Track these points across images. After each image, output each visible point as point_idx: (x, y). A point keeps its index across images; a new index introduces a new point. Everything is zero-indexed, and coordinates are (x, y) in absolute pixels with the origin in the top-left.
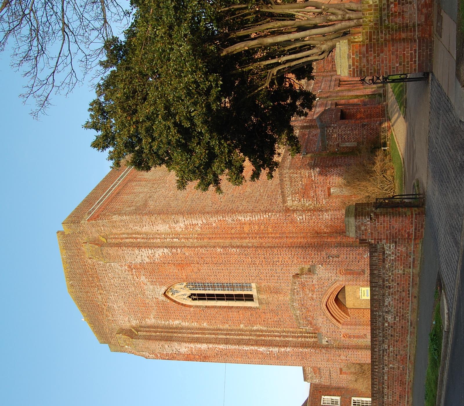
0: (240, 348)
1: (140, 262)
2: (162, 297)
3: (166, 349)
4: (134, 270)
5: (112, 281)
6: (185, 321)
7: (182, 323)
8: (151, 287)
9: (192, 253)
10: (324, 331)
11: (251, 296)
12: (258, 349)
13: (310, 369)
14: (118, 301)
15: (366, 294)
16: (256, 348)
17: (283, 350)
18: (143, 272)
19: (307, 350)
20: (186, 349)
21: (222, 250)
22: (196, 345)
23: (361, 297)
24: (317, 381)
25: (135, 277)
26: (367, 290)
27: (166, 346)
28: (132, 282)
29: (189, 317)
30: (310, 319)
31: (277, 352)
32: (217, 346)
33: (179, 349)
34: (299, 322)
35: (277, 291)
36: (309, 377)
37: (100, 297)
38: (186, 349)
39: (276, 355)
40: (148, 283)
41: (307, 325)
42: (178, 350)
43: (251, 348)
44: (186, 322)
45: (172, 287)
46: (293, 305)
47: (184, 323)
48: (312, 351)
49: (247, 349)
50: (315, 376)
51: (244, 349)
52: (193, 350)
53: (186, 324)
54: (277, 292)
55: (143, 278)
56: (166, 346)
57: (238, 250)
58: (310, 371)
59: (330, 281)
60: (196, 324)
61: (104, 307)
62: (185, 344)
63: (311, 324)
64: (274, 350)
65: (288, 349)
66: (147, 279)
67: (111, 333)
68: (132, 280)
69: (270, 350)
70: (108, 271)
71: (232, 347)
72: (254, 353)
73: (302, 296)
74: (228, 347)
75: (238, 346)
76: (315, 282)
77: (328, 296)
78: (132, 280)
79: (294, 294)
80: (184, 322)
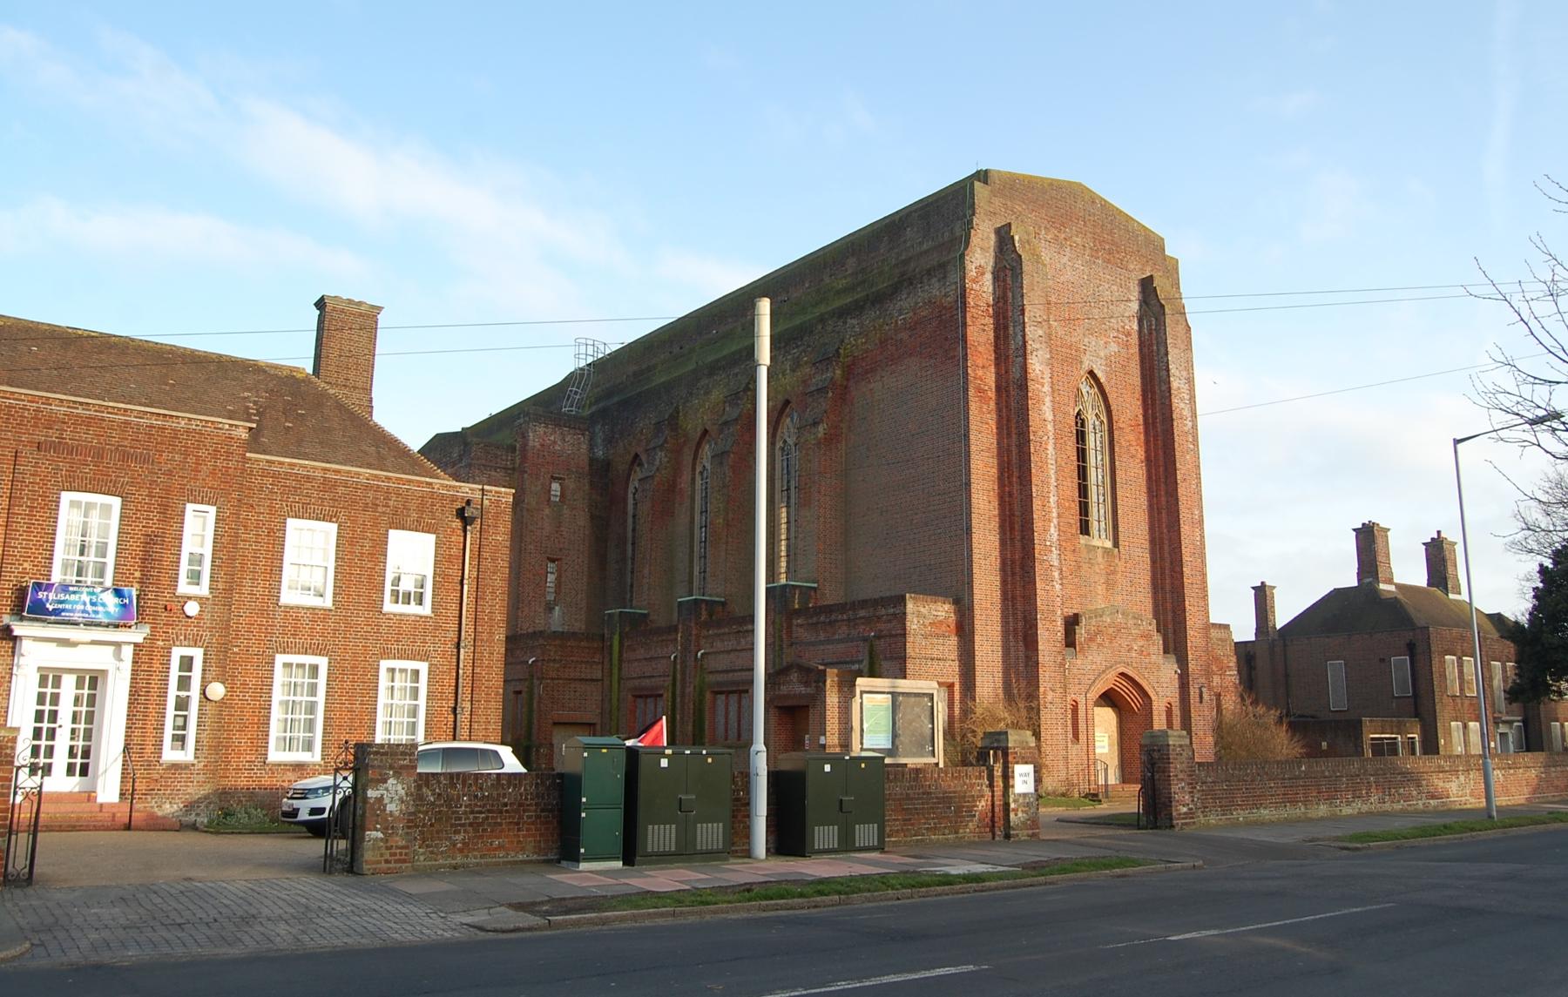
0: (1051, 488)
1: (1172, 371)
2: (1087, 365)
3: (1036, 328)
4: (1125, 339)
5: (1107, 286)
8: (1102, 354)
9: (1190, 467)
10: (1079, 662)
11: (1087, 533)
12: (1052, 525)
13: (939, 614)
14: (1074, 273)
16: (1055, 521)
17: (1056, 574)
18: (1123, 351)
19: (1059, 623)
21: (1197, 517)
24: (915, 627)
25: (1115, 334)
26: (1104, 747)
27: (1040, 332)
28: (1108, 323)
30: (1099, 640)
31: (1052, 563)
32: (1051, 441)
34: (1090, 618)
35: (1110, 585)
36: (922, 610)
37: (1079, 240)
39: (1045, 558)
40: (1107, 351)
41: (1088, 632)
42: (1035, 353)
43: (1054, 510)
45: (1096, 390)
46: (1117, 612)
48: (1059, 634)
49: (1051, 500)
50: (927, 622)
51: (1051, 495)
52: (1040, 387)
54: (1107, 583)
55: (1114, 348)
57: (1198, 543)
58: (936, 613)
59: (1156, 685)
61: (1063, 236)
63: (1091, 640)
64: (1055, 556)
65: (1058, 587)
66: (1113, 353)
67: (1015, 213)
68: (1111, 324)
69: (1054, 549)
70: (1120, 289)
71: (1053, 471)
72: (1044, 513)
73: (1133, 632)
74: (1052, 464)
75: (1055, 484)
76: (1154, 657)
77: (1137, 678)
78: (1111, 324)
79: (1135, 618)
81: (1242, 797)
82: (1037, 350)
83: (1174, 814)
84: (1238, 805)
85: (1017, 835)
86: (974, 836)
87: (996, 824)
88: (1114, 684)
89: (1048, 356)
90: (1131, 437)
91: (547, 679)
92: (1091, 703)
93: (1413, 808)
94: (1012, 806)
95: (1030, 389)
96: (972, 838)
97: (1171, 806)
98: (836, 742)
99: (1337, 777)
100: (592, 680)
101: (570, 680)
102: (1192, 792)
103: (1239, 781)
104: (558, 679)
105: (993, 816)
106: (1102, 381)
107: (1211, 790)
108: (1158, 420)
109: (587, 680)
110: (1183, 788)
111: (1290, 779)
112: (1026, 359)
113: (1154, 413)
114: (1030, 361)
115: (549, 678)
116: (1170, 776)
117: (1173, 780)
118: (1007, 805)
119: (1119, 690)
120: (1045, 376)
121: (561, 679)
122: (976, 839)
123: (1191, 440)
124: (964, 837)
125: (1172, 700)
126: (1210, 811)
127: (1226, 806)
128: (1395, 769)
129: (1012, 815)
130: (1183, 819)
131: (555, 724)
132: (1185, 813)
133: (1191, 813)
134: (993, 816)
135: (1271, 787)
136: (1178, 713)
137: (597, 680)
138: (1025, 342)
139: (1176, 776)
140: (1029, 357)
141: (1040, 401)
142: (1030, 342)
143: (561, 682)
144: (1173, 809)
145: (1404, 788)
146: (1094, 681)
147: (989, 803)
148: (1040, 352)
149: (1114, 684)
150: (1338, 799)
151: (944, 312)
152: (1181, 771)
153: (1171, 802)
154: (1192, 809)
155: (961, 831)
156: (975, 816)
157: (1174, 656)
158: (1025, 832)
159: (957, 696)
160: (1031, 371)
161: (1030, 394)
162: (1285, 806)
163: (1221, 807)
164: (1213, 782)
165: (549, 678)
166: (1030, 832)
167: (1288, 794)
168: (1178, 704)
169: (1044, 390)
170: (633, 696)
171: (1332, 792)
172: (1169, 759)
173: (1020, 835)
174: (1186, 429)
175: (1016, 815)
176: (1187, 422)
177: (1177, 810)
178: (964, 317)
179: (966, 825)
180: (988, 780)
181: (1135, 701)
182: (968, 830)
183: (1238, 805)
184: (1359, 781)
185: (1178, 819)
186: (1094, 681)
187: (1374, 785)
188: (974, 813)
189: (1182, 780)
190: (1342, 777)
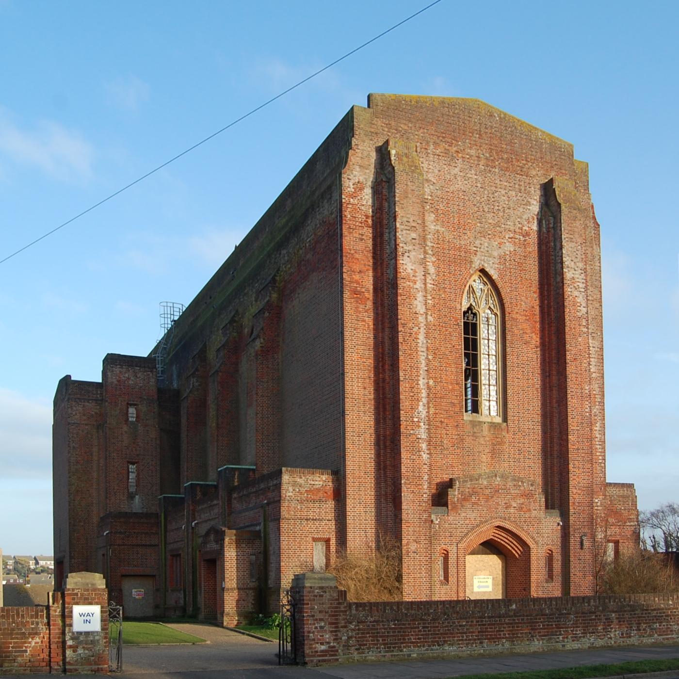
6: (434, 285)
7: (430, 278)
15: (482, 584)
20: (409, 271)
22: (421, 293)
23: (476, 577)
29: (443, 296)
33: (408, 257)
38: (411, 271)
42: (407, 254)
44: (433, 286)
47: (430, 282)
52: (411, 284)
53: (430, 286)
56: (414, 235)
60: (430, 302)
62: (423, 273)
80: (433, 283)
81: (416, 635)
82: (409, 251)
83: (307, 651)
84: (413, 643)
85: (76, 670)
86: (25, 670)
87: (52, 660)
88: (493, 536)
89: (422, 257)
90: (526, 326)
91: (114, 545)
92: (461, 552)
93: (671, 641)
94: (70, 643)
95: (400, 286)
96: (22, 672)
97: (304, 644)
98: (235, 585)
99: (563, 614)
100: (151, 546)
101: (133, 545)
102: (336, 631)
103: (414, 620)
104: (123, 545)
105: (50, 652)
106: (494, 278)
107: (372, 629)
108: (552, 309)
109: (146, 545)
110: (321, 627)
111: (489, 617)
112: (396, 260)
113: (549, 303)
114: (401, 262)
115: (117, 545)
116: (304, 617)
117: (308, 620)
118: (64, 642)
119: (499, 540)
120: (417, 274)
121: (126, 545)
122: (28, 672)
123: (585, 324)
124: (11, 670)
125: (553, 548)
126: (369, 648)
127: (391, 644)
128: (648, 605)
129: (69, 652)
130: (320, 656)
131: (123, 576)
132: (322, 651)
133: (332, 651)
134: (50, 652)
135: (460, 626)
136: (560, 558)
137: (155, 545)
138: (396, 245)
139: (313, 616)
140: (400, 258)
141: (411, 297)
142: (401, 245)
143: (126, 547)
144: (306, 647)
145: (661, 622)
146: (467, 534)
147: (47, 636)
148: (412, 254)
149: (493, 536)
150: (560, 635)
151: (331, 228)
152: (320, 612)
153: (304, 640)
154: (334, 647)
155: (6, 665)
156: (26, 651)
157: (558, 511)
158: (87, 667)
159: (333, 548)
160: (401, 271)
161: (400, 291)
162: (481, 643)
163: (384, 644)
164: (374, 621)
165: (117, 545)
166: (95, 667)
167: (485, 632)
168: (559, 550)
169: (415, 286)
170: (171, 555)
171: (553, 628)
172: (303, 600)
173: (80, 670)
174: (579, 314)
175: (74, 651)
176: (582, 308)
177: (311, 648)
178: (341, 229)
179: (14, 660)
180: (46, 618)
181: (516, 549)
182: (16, 664)
183: (413, 643)
184: (594, 617)
185: (314, 656)
186: (467, 534)
187: (615, 621)
188: (24, 648)
189: (321, 620)
190: (570, 614)
